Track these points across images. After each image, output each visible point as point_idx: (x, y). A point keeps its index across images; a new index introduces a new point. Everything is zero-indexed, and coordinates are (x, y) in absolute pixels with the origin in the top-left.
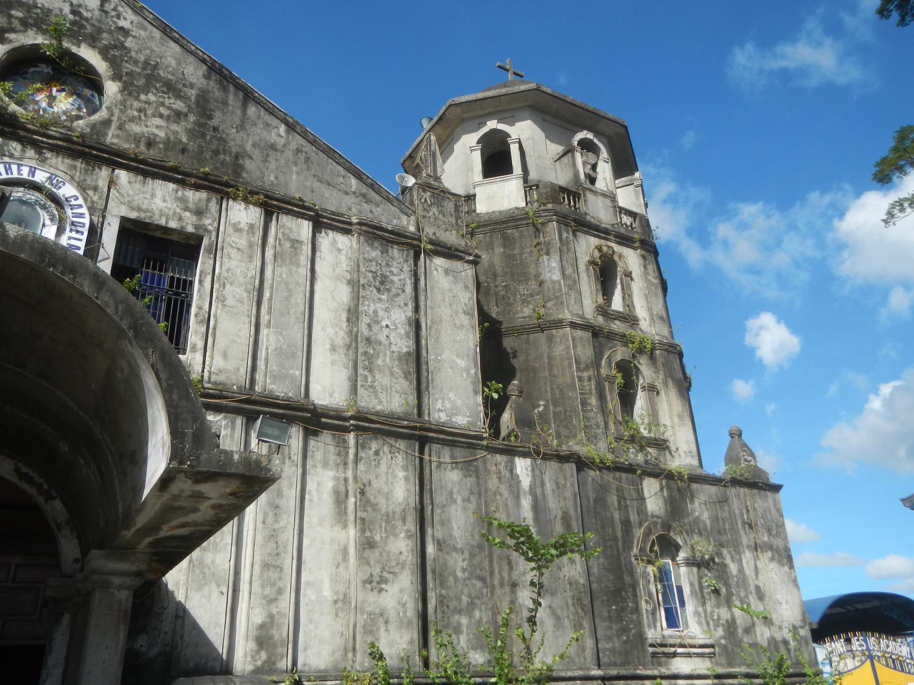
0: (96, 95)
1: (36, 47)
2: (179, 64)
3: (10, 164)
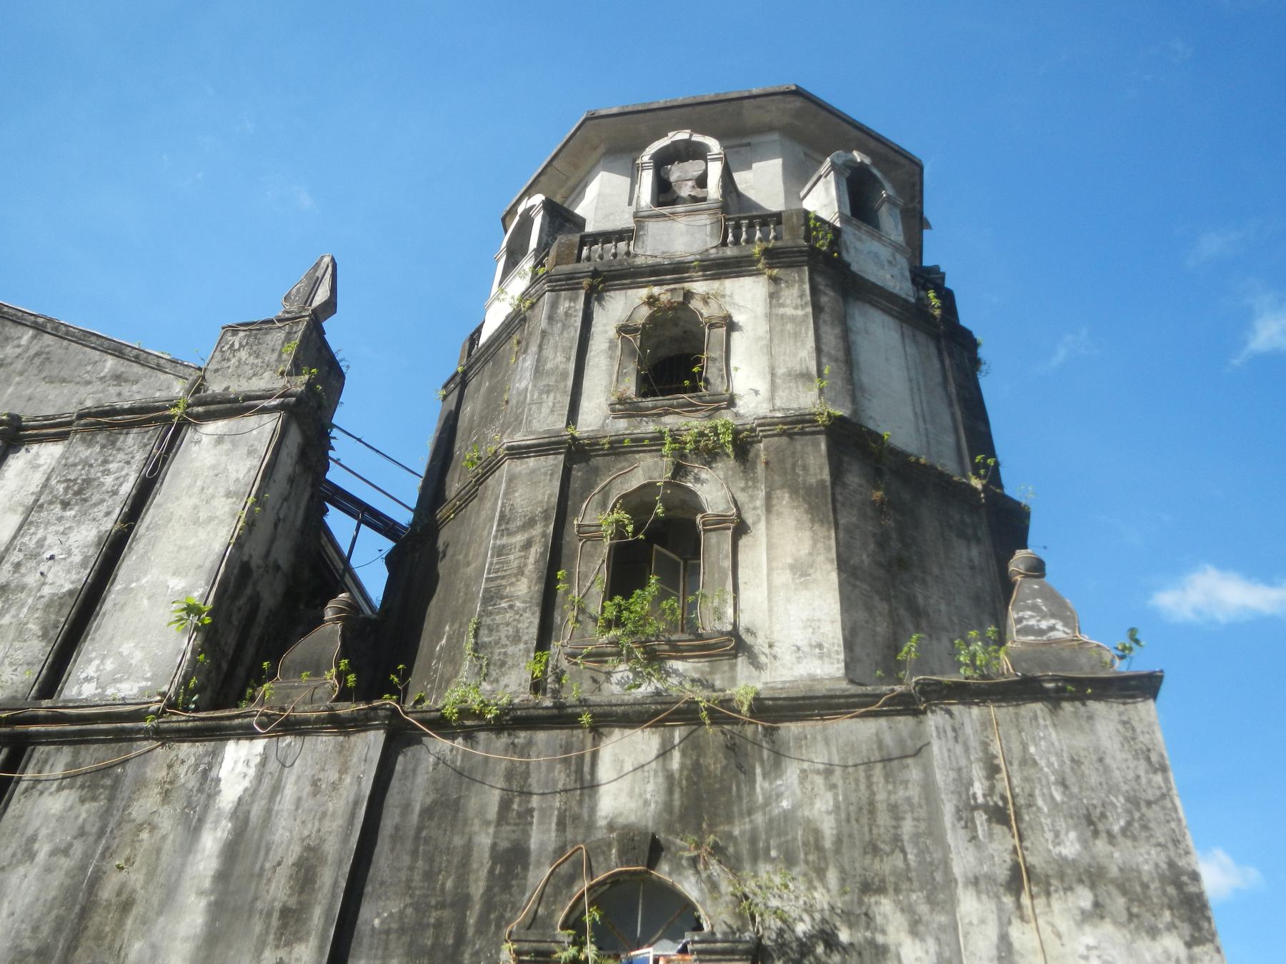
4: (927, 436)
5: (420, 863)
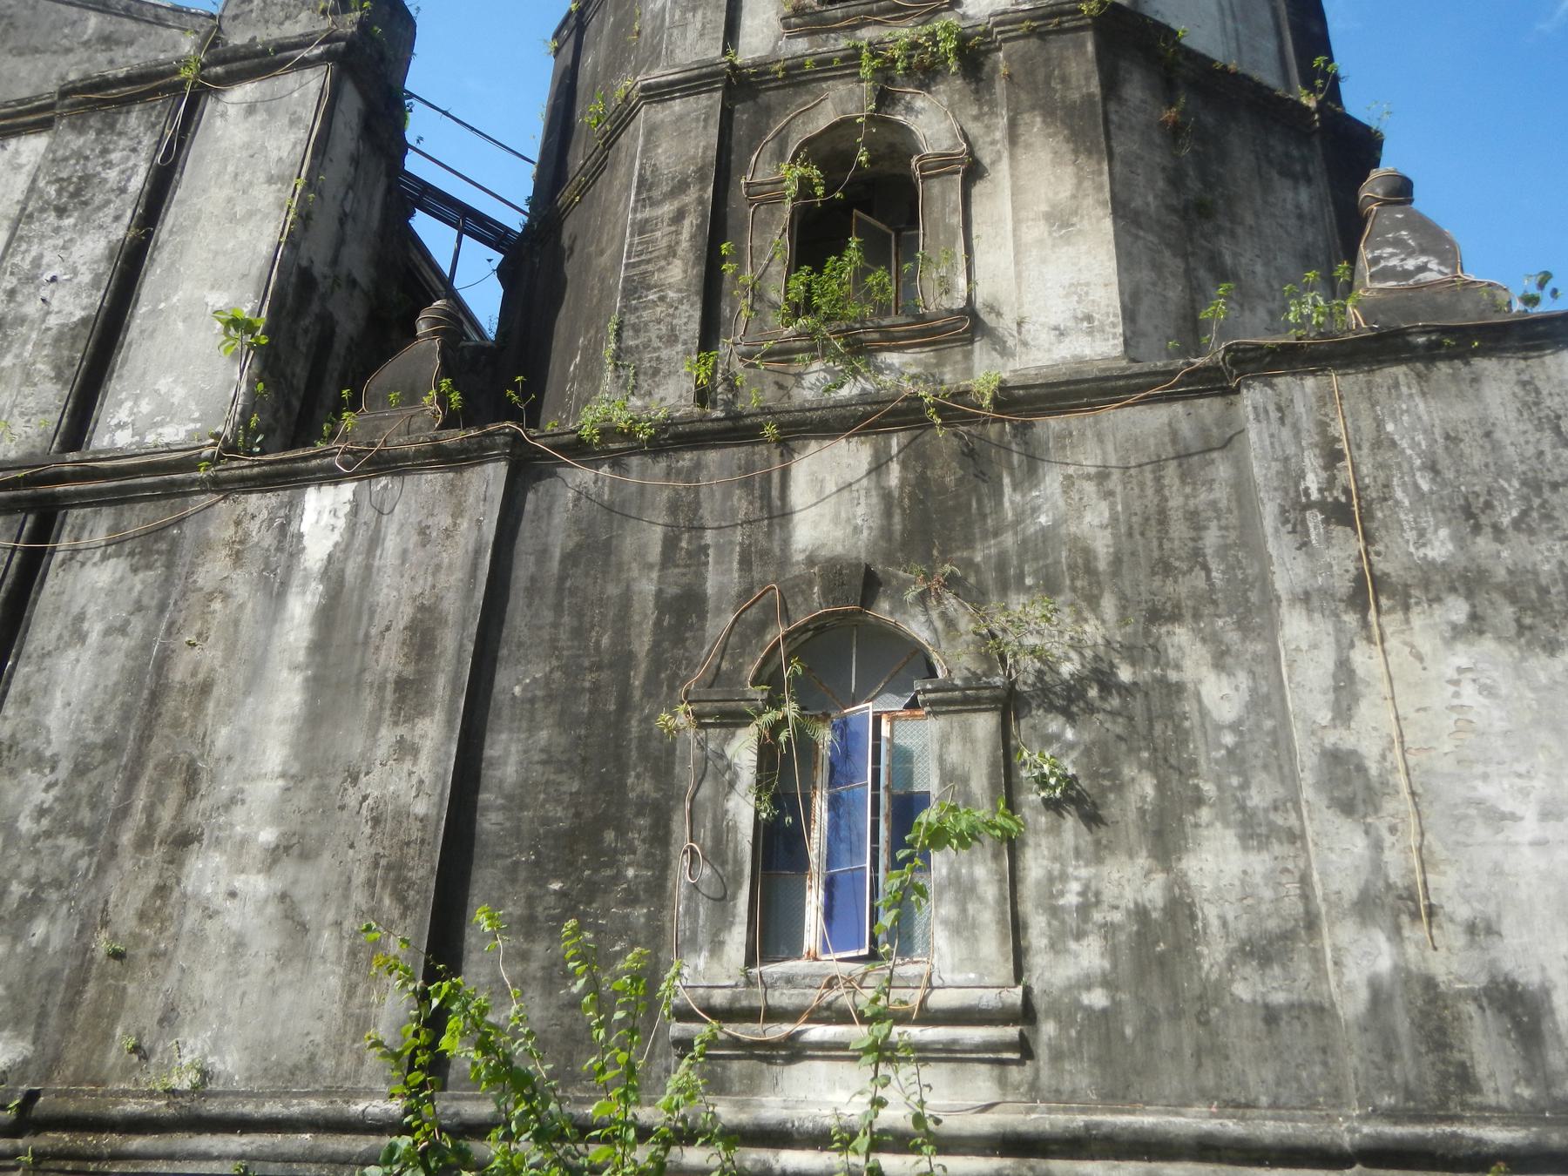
4: (1237, 39)
5: (566, 619)
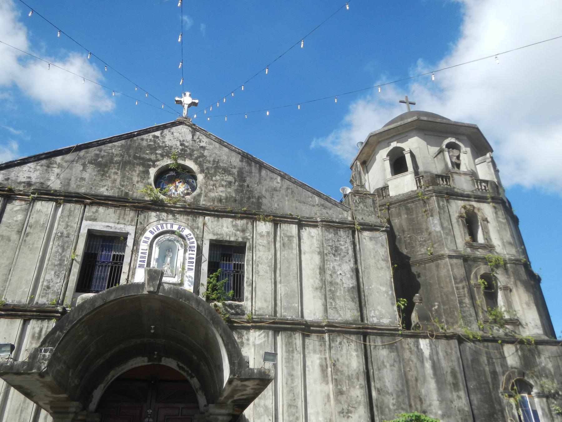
0: (194, 181)
1: (168, 165)
2: (228, 158)
3: (162, 224)
5: (475, 373)
